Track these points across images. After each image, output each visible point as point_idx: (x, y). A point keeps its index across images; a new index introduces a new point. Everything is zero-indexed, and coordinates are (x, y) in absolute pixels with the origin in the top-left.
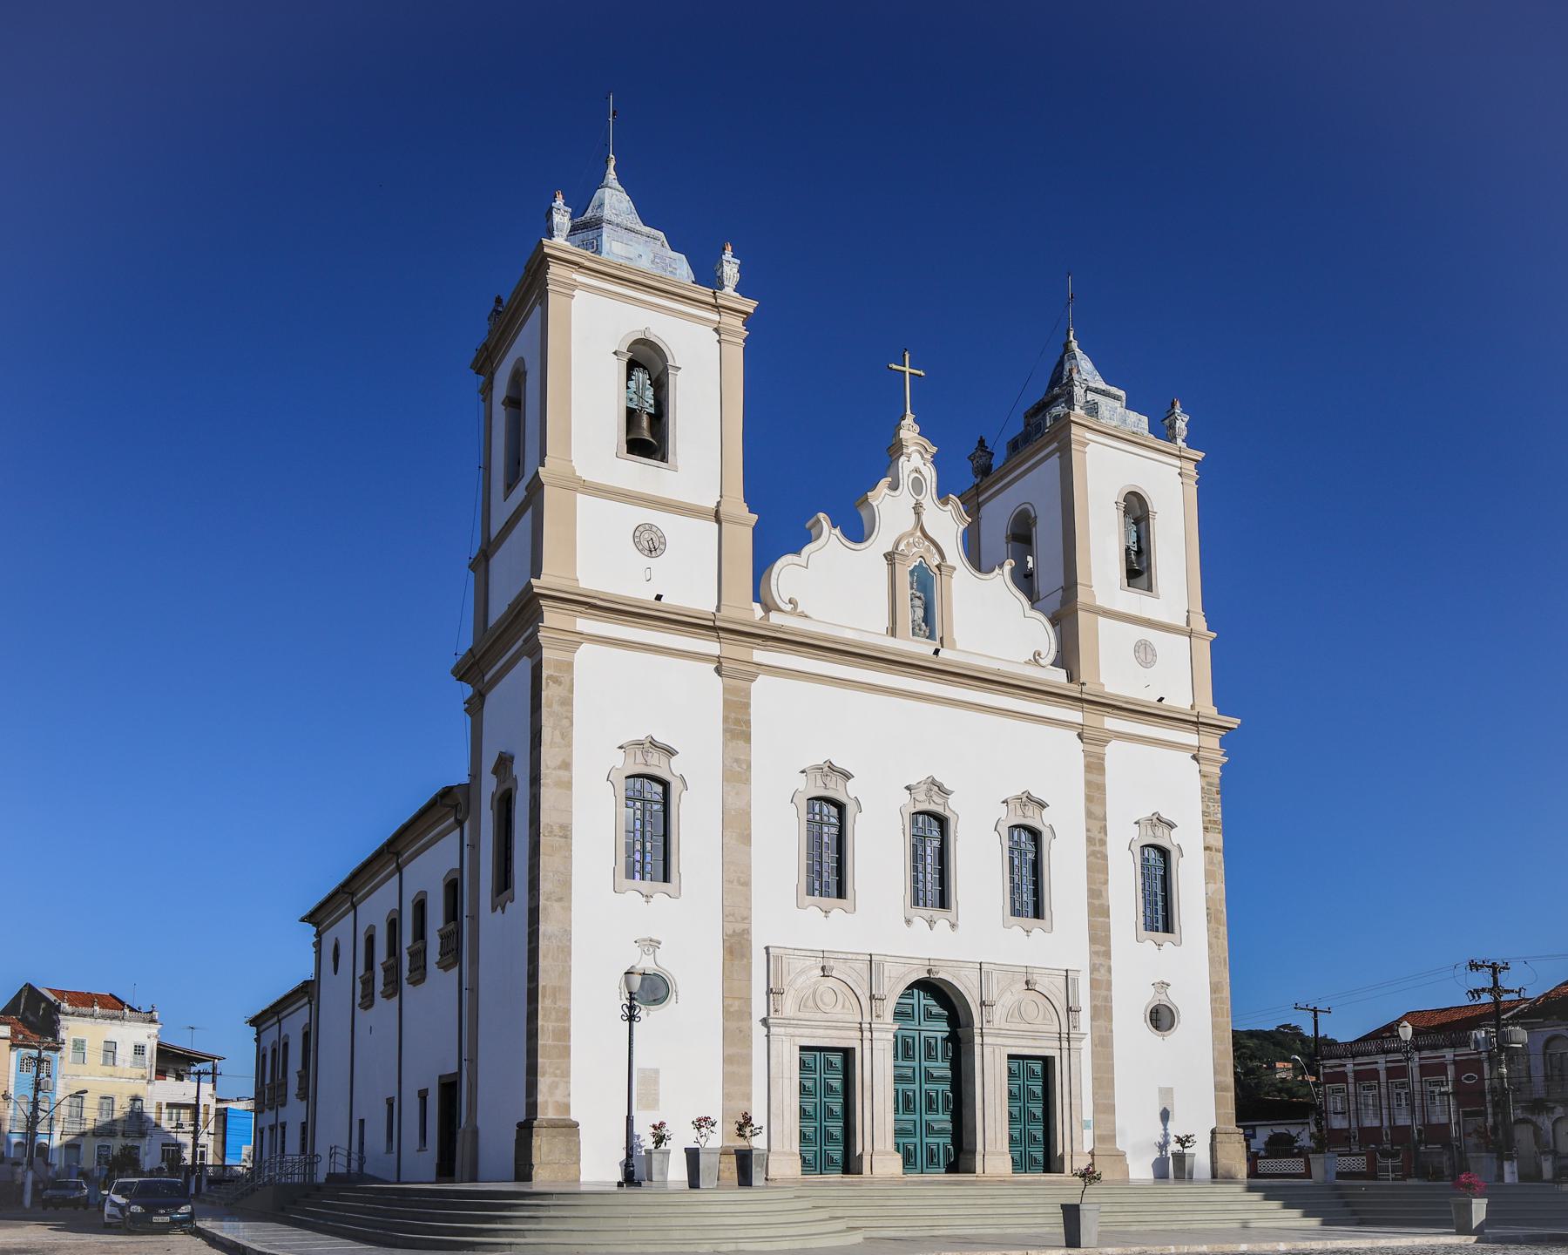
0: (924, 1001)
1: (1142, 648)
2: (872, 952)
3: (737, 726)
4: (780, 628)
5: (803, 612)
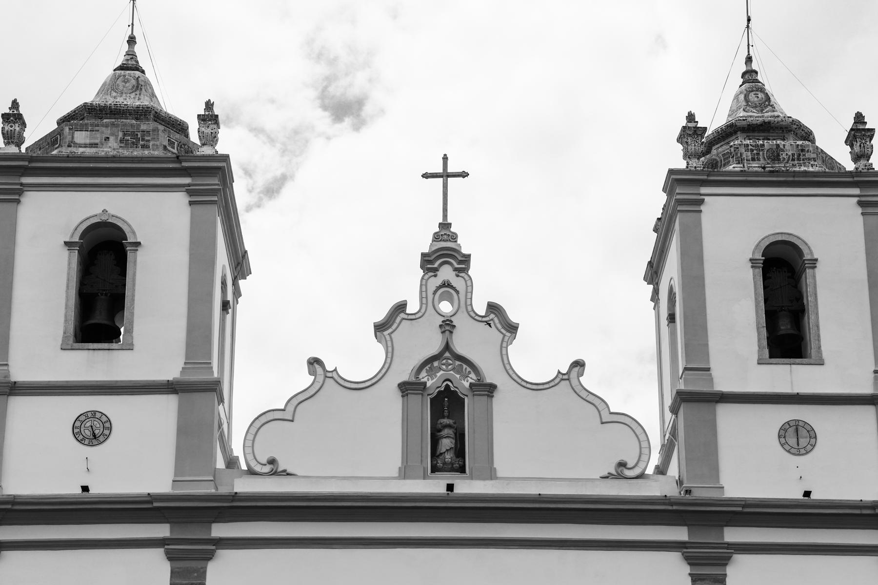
1: (791, 431)
4: (235, 497)
5: (285, 471)
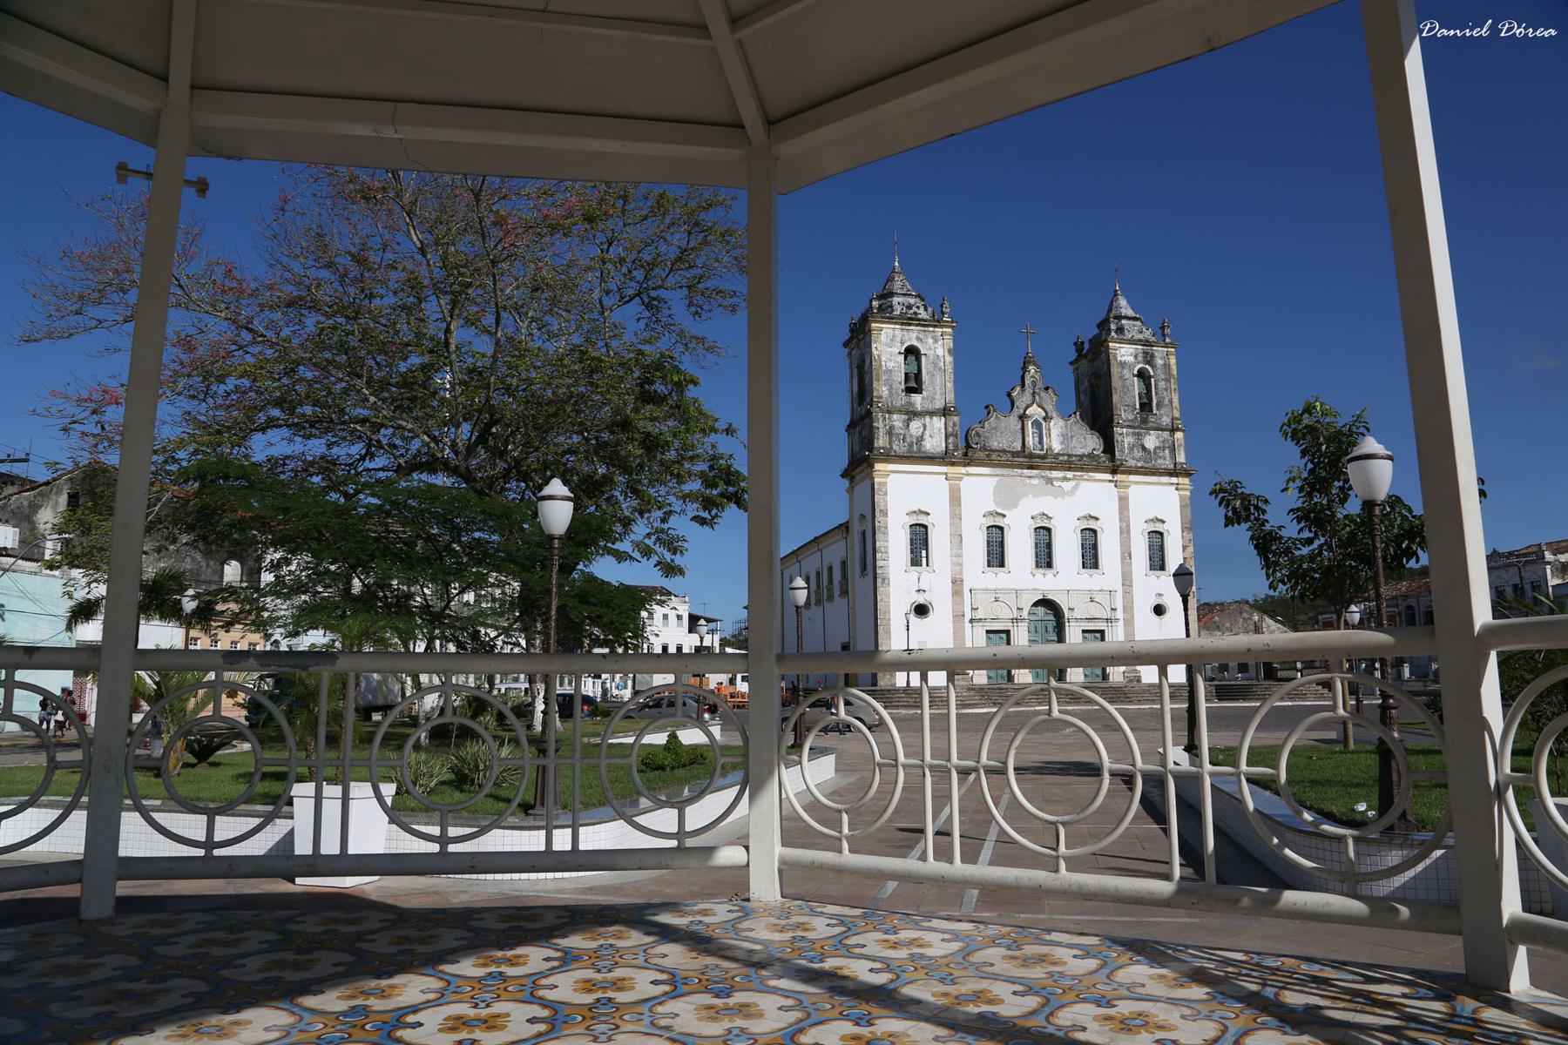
0: (1041, 610)
2: (1017, 588)
3: (955, 499)
